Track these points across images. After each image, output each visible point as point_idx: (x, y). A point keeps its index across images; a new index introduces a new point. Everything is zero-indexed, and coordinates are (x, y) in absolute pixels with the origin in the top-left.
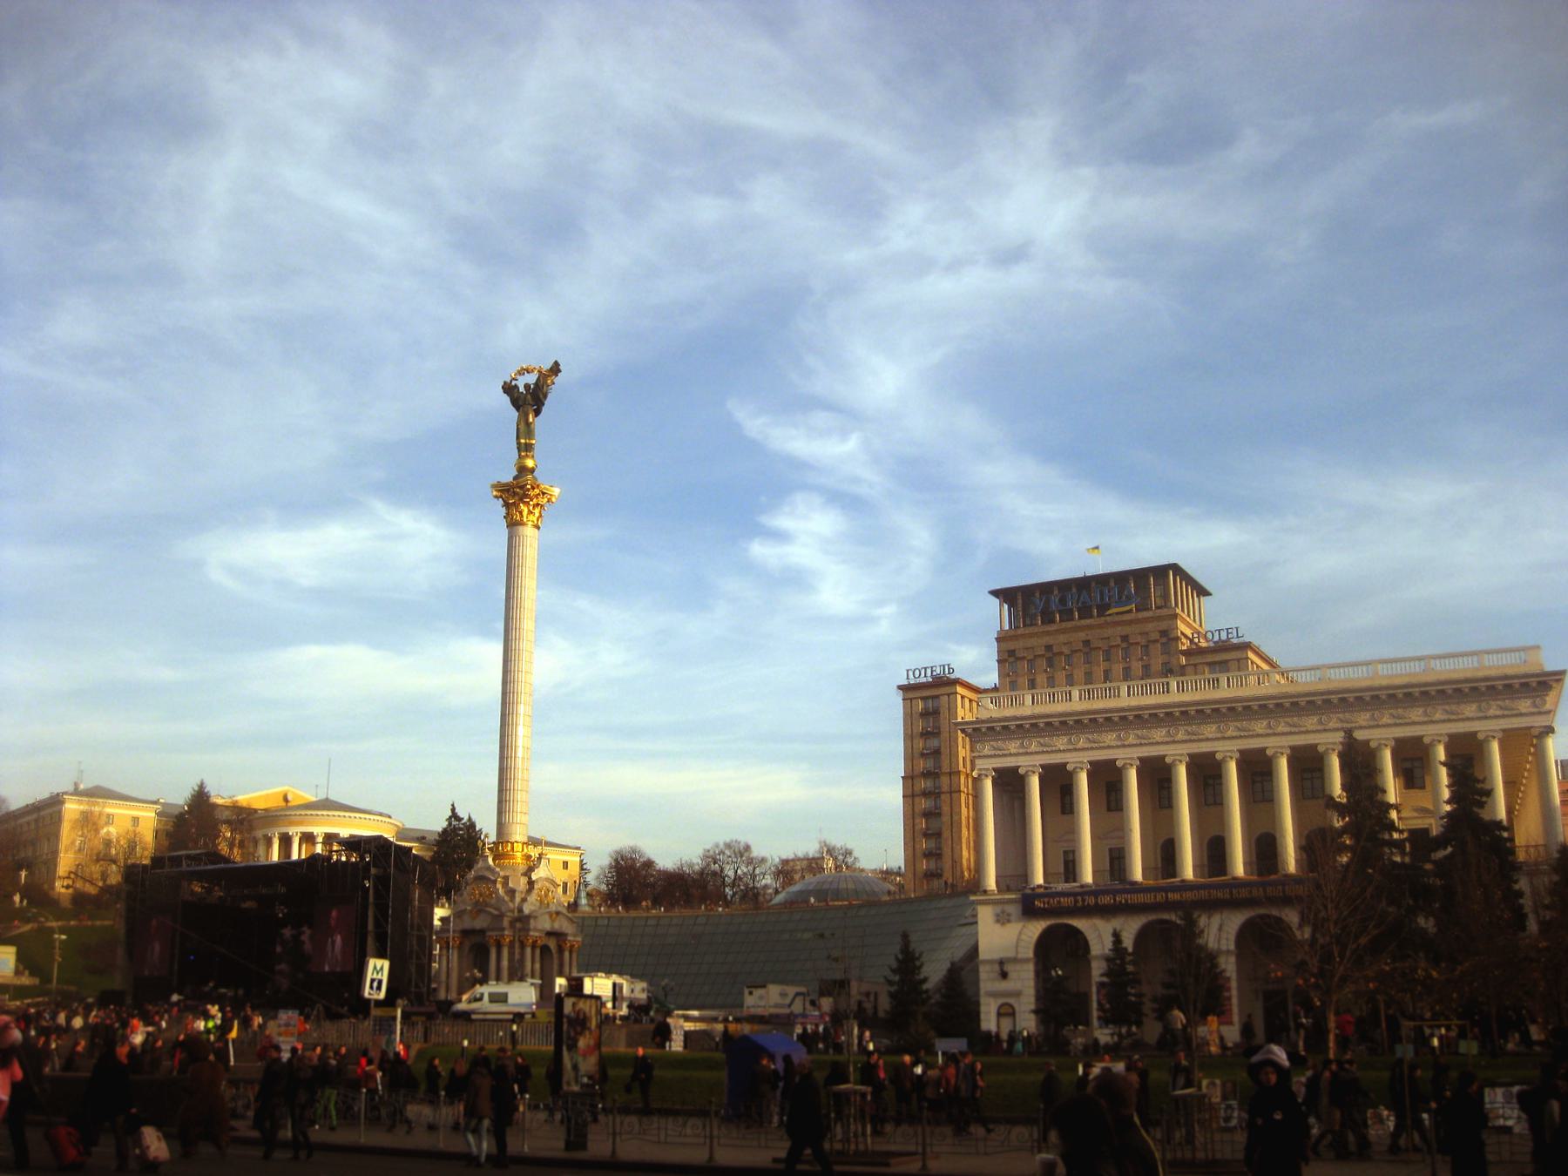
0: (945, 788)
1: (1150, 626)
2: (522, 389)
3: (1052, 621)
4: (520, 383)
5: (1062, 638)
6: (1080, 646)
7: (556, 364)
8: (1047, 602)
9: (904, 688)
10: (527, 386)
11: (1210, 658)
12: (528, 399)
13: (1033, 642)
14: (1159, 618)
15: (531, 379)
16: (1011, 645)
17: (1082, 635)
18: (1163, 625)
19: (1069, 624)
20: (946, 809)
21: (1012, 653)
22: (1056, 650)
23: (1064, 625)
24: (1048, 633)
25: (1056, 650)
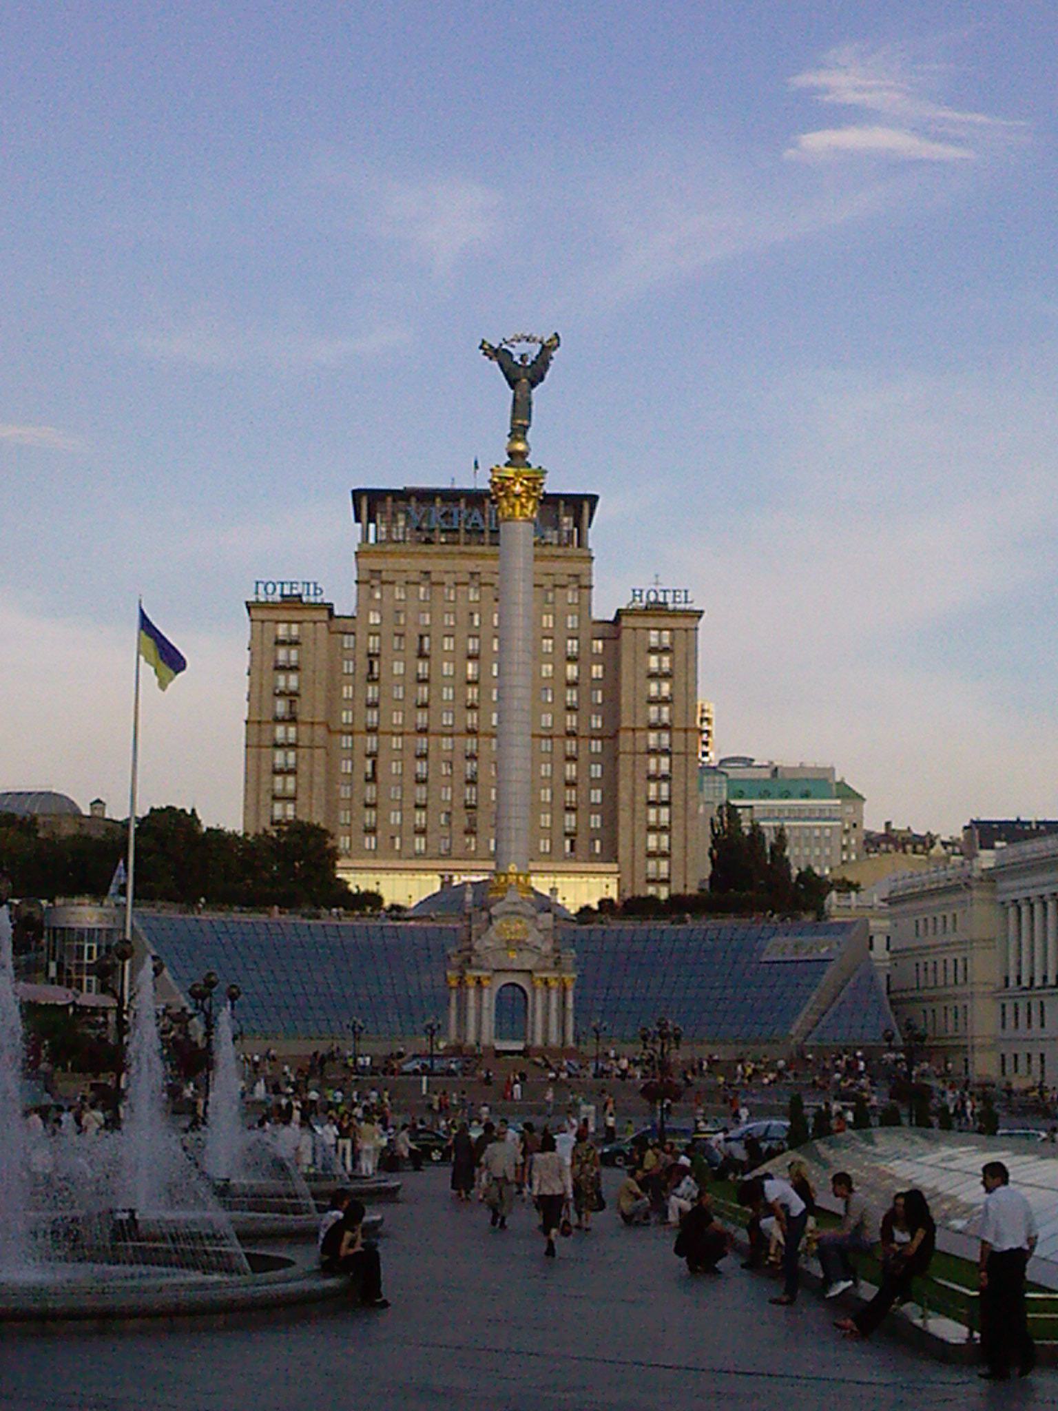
0: (304, 741)
1: (557, 566)
2: (517, 358)
3: (428, 542)
4: (516, 351)
5: (444, 564)
6: (466, 578)
7: (556, 334)
8: (427, 516)
9: (249, 606)
10: (523, 357)
11: (651, 622)
12: (524, 374)
13: (405, 563)
14: (568, 558)
15: (534, 350)
16: (376, 564)
17: (471, 565)
18: (575, 567)
19: (455, 548)
20: (303, 768)
21: (375, 573)
22: (434, 577)
23: (448, 548)
24: (426, 555)
25: (434, 577)
